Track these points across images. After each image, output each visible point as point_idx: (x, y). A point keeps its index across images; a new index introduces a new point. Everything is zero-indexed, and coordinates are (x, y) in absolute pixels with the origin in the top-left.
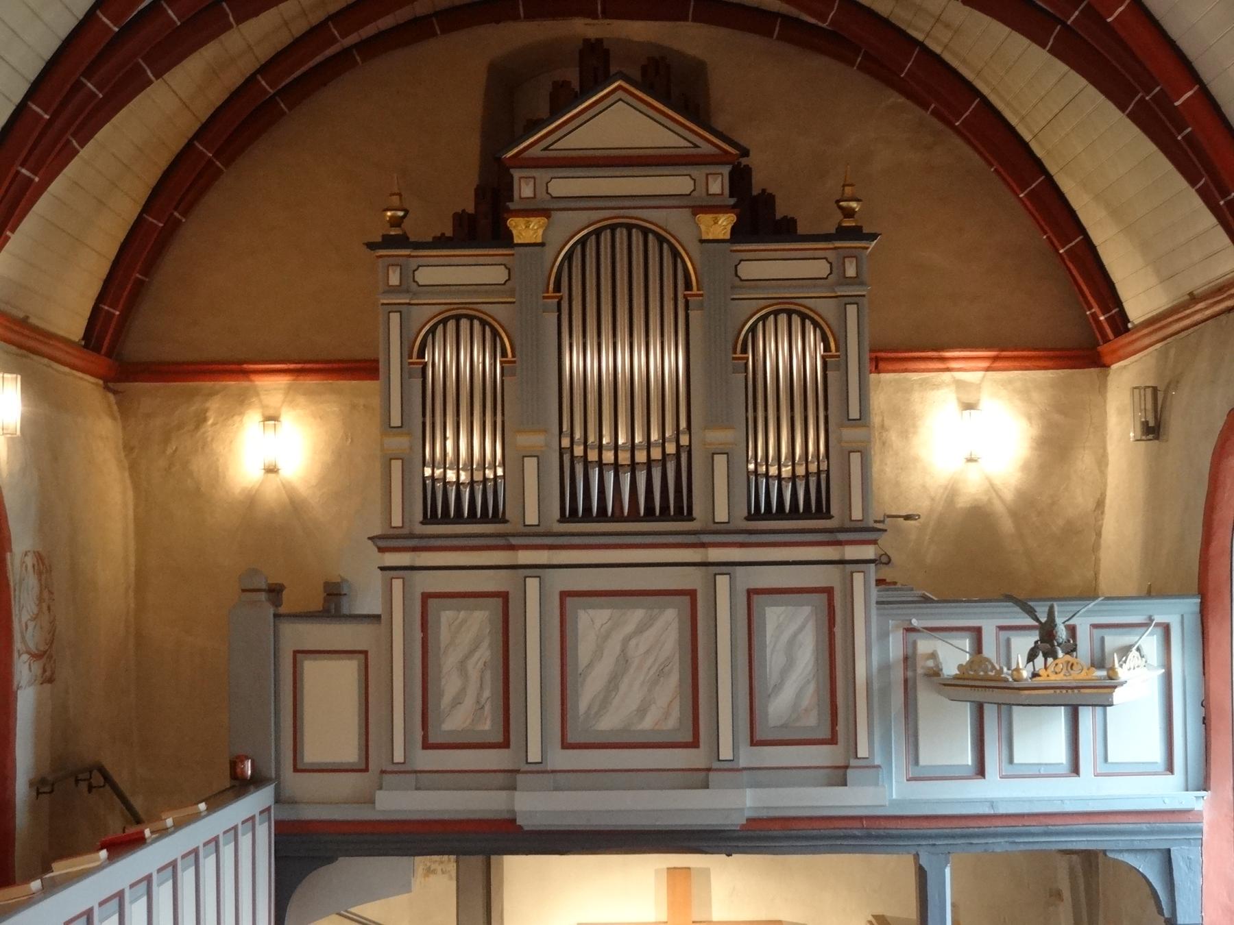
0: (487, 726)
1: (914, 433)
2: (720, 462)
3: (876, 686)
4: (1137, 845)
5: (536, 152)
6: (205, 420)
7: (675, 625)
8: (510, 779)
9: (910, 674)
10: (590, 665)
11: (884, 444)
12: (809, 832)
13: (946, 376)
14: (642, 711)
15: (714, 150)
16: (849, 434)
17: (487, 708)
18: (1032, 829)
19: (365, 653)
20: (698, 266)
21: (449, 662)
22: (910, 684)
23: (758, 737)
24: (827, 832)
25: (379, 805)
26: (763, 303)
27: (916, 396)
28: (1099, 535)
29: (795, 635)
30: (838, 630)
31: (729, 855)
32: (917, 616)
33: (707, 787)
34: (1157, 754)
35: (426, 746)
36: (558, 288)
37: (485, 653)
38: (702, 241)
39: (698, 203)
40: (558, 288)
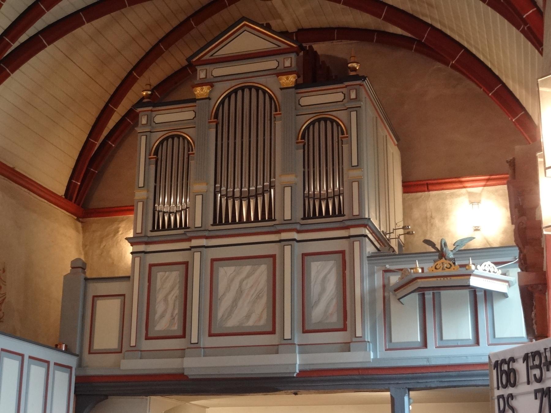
0: (175, 327)
1: (448, 219)
2: (288, 190)
3: (367, 299)
5: (207, 57)
6: (118, 232)
7: (266, 273)
8: (182, 353)
10: (224, 294)
11: (432, 225)
12: (332, 378)
13: (463, 191)
14: (248, 317)
15: (288, 47)
16: (354, 173)
17: (176, 318)
18: (451, 374)
19: (124, 295)
20: (280, 101)
21: (160, 296)
24: (341, 377)
25: (122, 367)
26: (312, 115)
27: (448, 201)
29: (325, 277)
30: (347, 272)
31: (296, 394)
32: (388, 263)
33: (277, 352)
35: (147, 338)
36: (216, 117)
37: (177, 292)
38: (281, 89)
39: (278, 72)
40: (216, 117)
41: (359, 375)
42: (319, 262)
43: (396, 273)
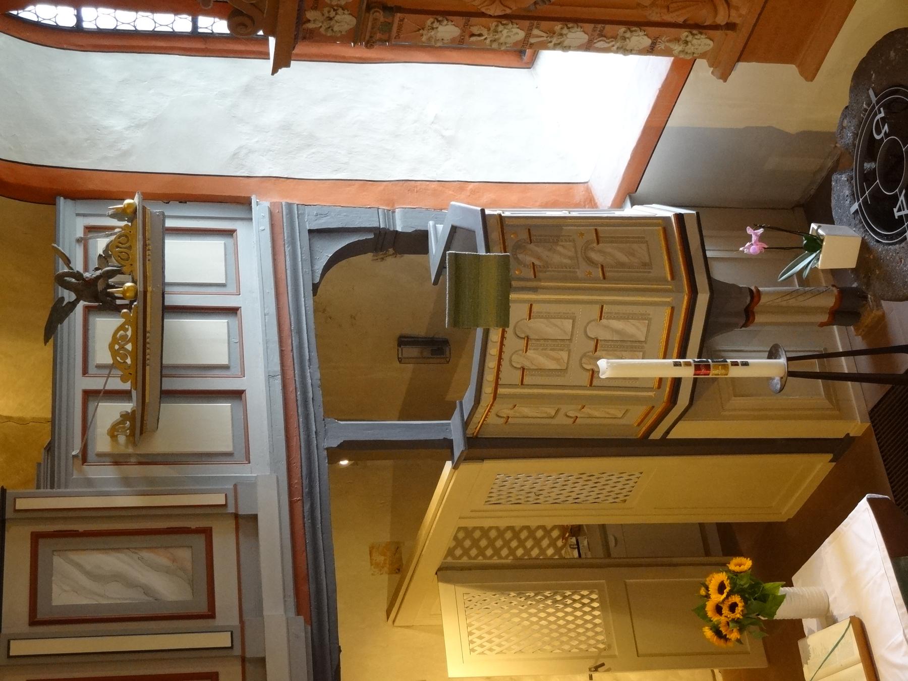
4: (307, 256)
9: (133, 460)
22: (143, 460)
23: (203, 608)
24: (308, 536)
28: (9, 419)
29: (88, 574)
30: (81, 527)
32: (67, 452)
33: (263, 660)
34: (217, 245)
41: (302, 500)
42: (54, 586)
43: (89, 442)
